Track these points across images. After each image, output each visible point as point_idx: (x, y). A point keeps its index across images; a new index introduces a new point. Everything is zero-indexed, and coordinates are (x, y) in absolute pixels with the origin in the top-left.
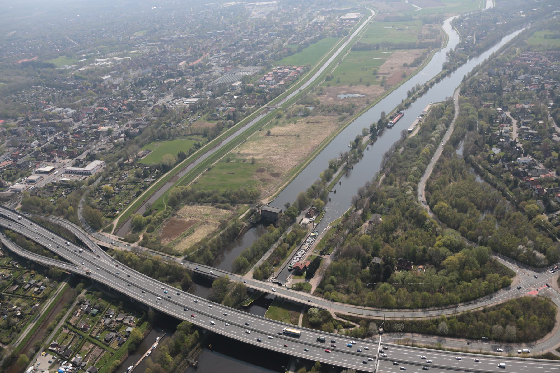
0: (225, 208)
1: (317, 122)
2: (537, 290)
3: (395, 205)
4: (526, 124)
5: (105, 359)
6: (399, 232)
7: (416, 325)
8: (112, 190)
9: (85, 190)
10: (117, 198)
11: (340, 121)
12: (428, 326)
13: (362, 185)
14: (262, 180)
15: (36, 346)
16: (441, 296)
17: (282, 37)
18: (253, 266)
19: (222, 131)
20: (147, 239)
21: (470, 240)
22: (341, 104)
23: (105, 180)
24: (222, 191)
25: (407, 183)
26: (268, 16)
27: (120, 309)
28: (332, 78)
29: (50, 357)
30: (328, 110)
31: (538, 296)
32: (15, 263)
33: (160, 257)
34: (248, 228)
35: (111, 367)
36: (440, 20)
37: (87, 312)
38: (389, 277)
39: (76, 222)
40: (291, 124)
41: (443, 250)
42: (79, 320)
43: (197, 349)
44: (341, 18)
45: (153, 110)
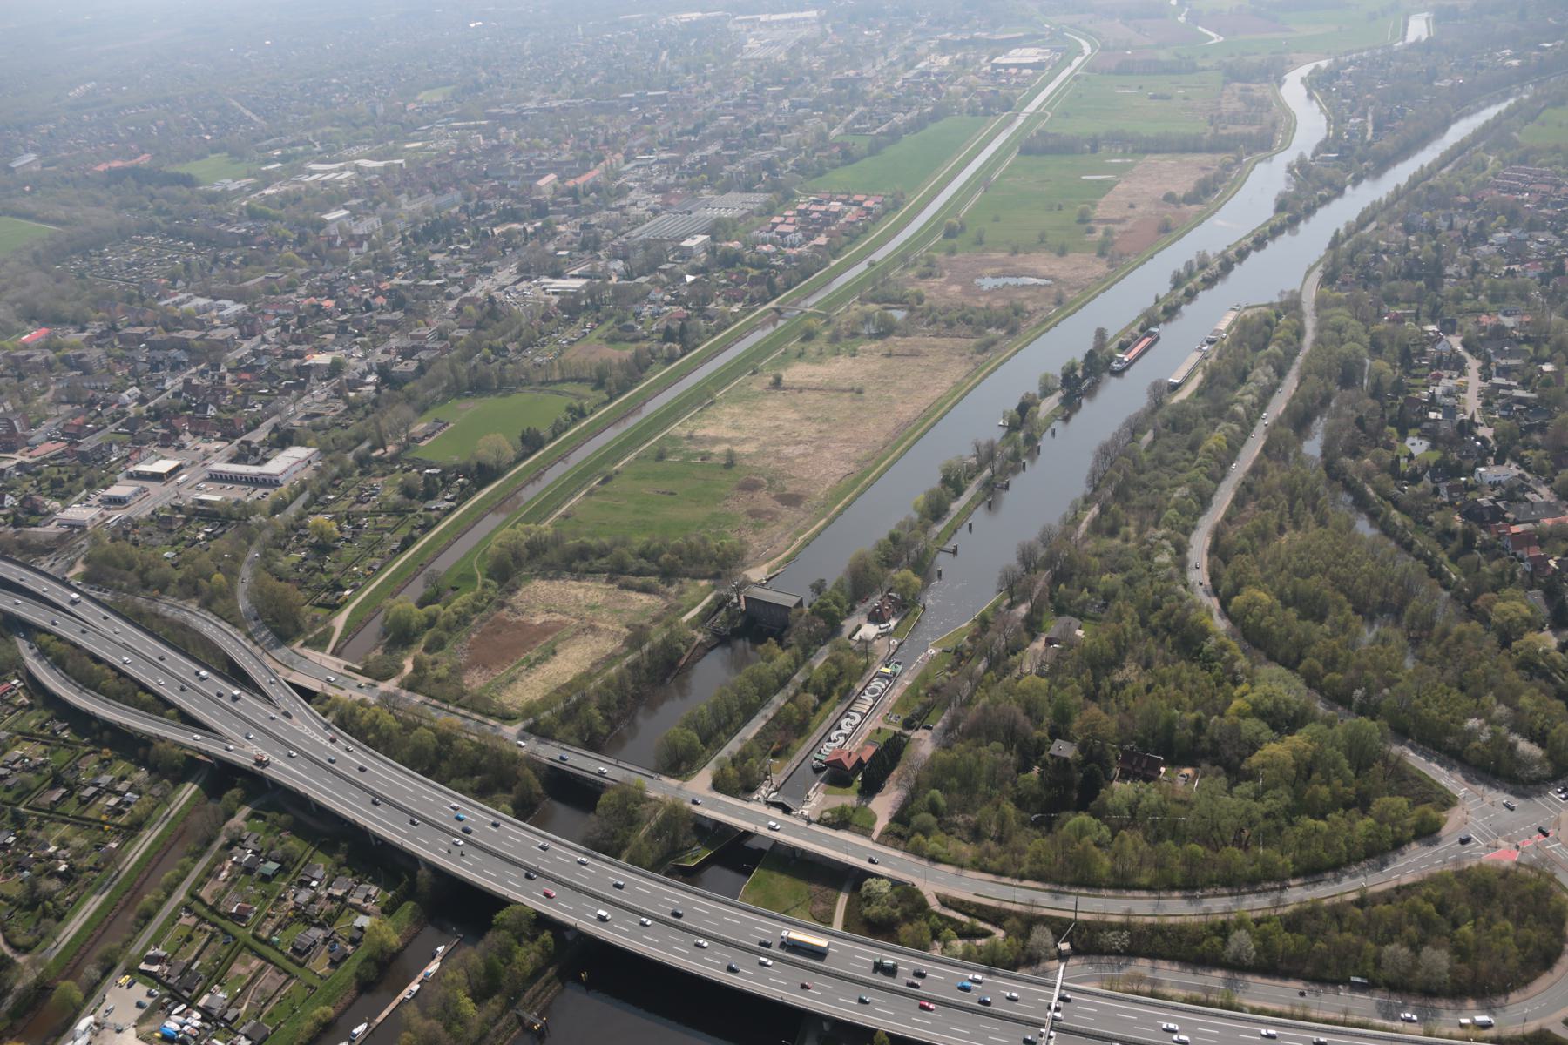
0: (645, 589)
1: (915, 354)
2: (1517, 847)
3: (1121, 593)
4: (1505, 371)
5: (291, 1001)
6: (1130, 672)
7: (1165, 938)
8: (335, 529)
9: (261, 527)
10: (348, 552)
11: (979, 353)
12: (1198, 943)
13: (1031, 535)
14: (753, 514)
15: (104, 959)
16: (1238, 854)
17: (826, 111)
18: (713, 754)
19: (649, 372)
20: (425, 670)
21: (1329, 698)
22: (983, 305)
23: (316, 502)
24: (639, 540)
25: (1160, 533)
26: (792, 51)
27: (339, 865)
28: (963, 229)
29: (140, 991)
30: (945, 321)
31: (1519, 864)
32: (58, 726)
33: (457, 721)
34: (706, 649)
35: (308, 1025)
36: (1274, 73)
37: (248, 871)
38: (1093, 798)
39: (230, 616)
40: (841, 358)
41: (1251, 726)
42: (226, 891)
43: (548, 982)
44: (995, 61)
45: (459, 309)
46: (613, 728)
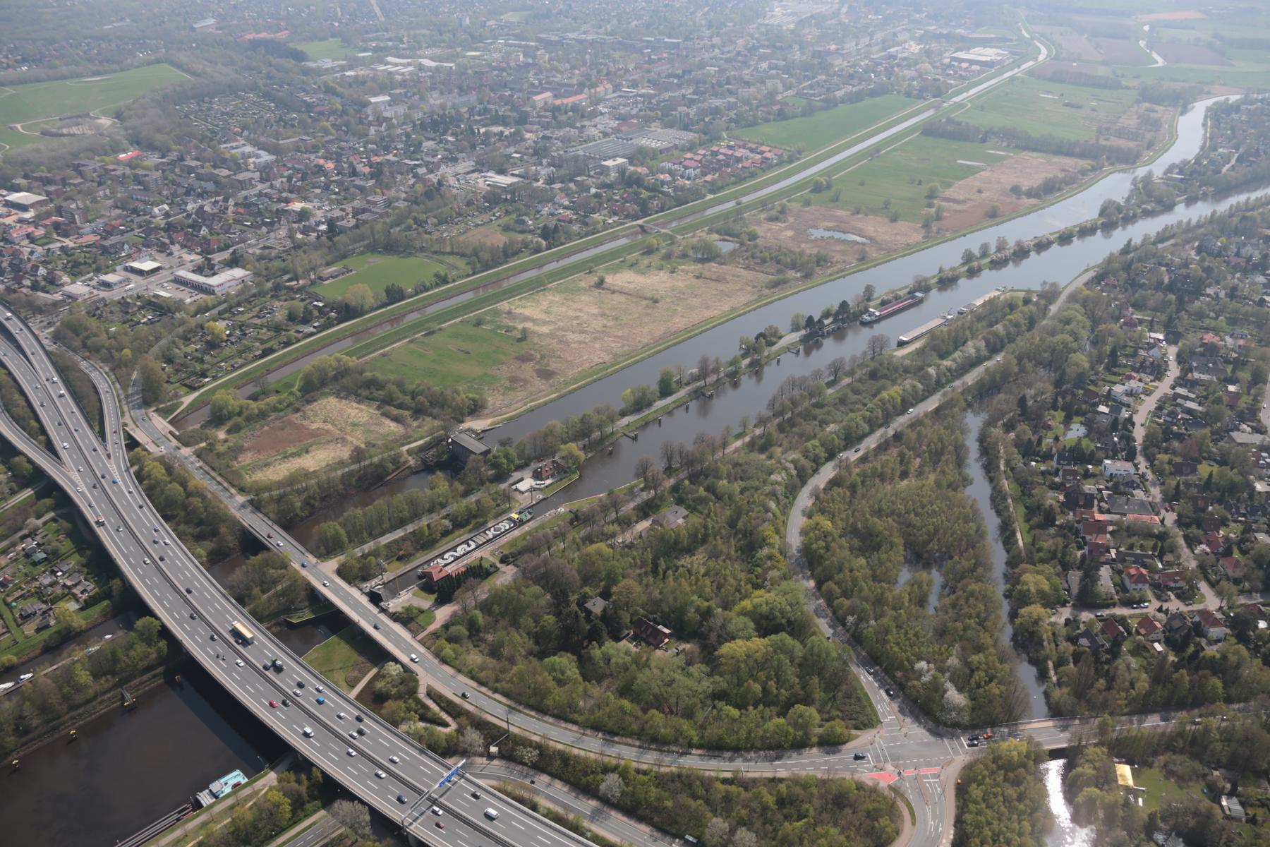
0: (396, 419)
1: (720, 279)
2: (900, 774)
4: (1192, 385)
6: (697, 561)
9: (182, 323)
12: (586, 774)
14: (513, 380)
26: (802, 23)
28: (829, 186)
34: (416, 472)
36: (1182, 101)
37: (27, 556)
40: (662, 273)
43: (154, 676)
46: (312, 514)
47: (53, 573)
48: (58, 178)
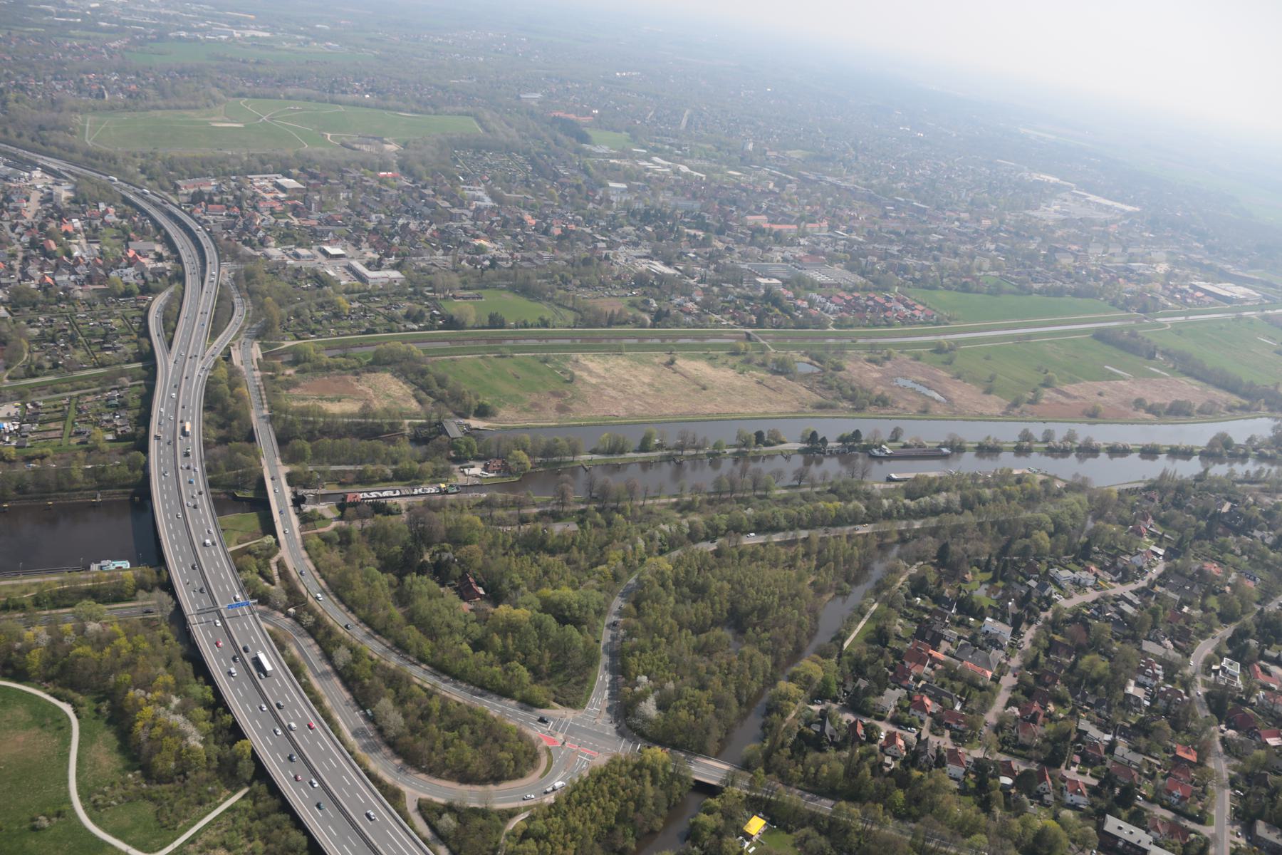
0: (420, 402)
43: (124, 493)
47: (115, 414)
48: (323, 176)
